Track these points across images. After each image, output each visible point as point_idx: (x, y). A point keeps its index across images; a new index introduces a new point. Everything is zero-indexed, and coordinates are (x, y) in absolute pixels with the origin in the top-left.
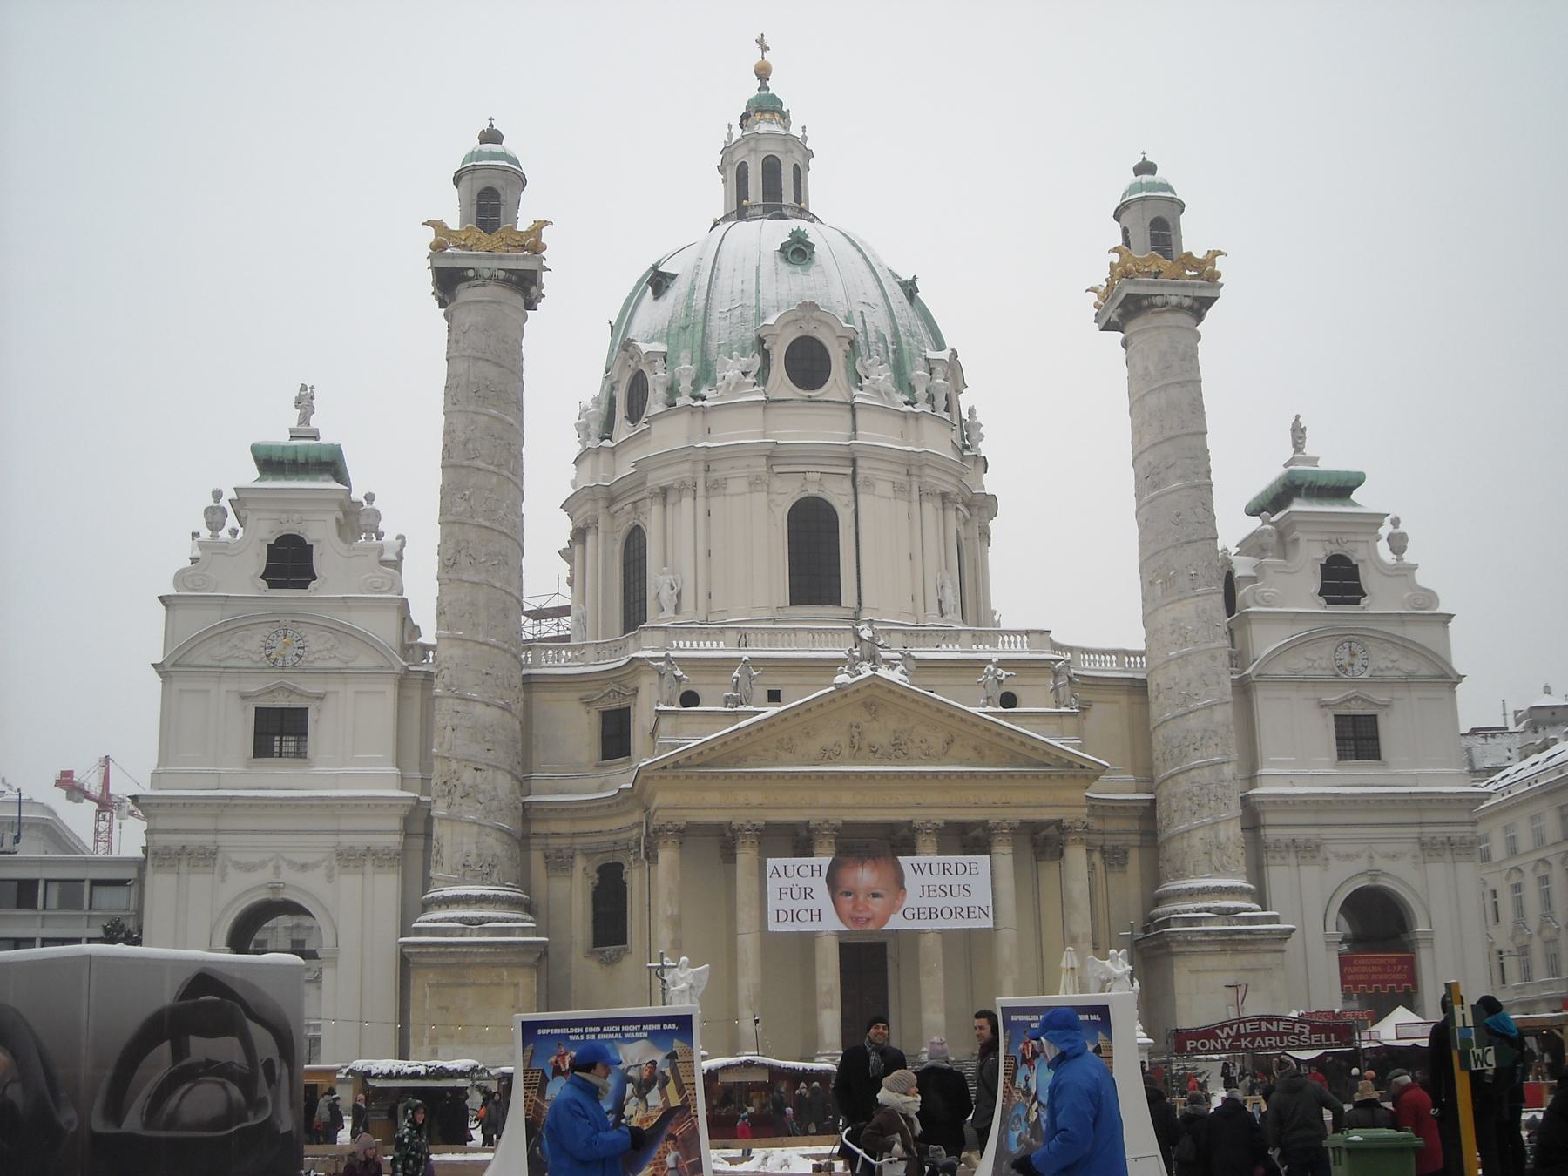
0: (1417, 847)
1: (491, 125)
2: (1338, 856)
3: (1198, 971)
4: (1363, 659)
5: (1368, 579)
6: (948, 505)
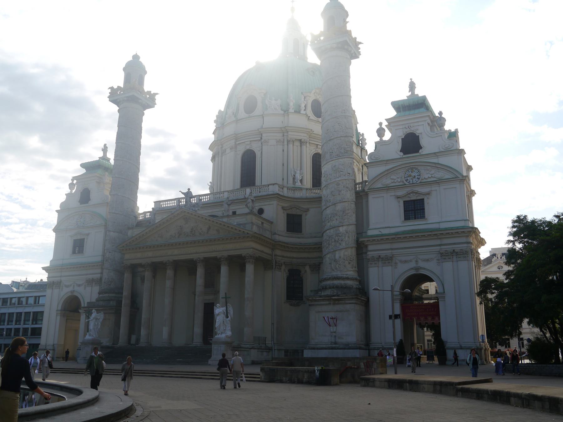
0: (439, 255)
1: (136, 53)
2: (401, 261)
3: (319, 312)
4: (418, 175)
5: (423, 142)
6: (302, 144)
